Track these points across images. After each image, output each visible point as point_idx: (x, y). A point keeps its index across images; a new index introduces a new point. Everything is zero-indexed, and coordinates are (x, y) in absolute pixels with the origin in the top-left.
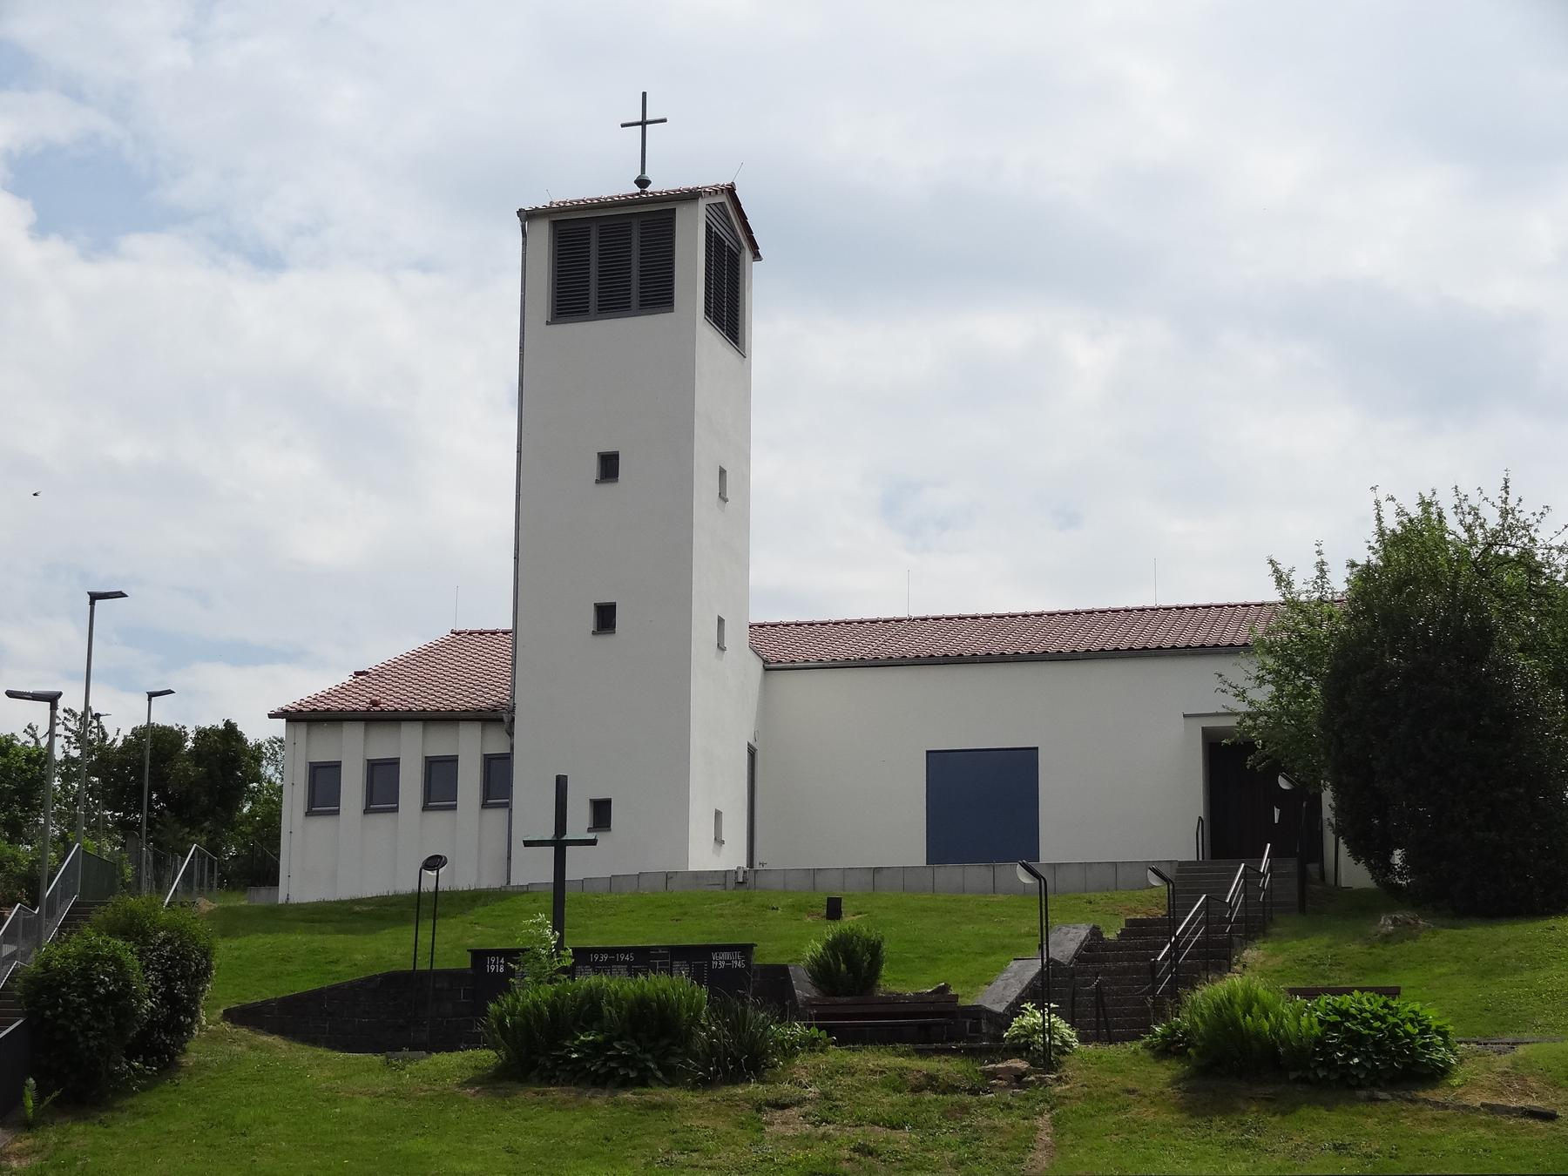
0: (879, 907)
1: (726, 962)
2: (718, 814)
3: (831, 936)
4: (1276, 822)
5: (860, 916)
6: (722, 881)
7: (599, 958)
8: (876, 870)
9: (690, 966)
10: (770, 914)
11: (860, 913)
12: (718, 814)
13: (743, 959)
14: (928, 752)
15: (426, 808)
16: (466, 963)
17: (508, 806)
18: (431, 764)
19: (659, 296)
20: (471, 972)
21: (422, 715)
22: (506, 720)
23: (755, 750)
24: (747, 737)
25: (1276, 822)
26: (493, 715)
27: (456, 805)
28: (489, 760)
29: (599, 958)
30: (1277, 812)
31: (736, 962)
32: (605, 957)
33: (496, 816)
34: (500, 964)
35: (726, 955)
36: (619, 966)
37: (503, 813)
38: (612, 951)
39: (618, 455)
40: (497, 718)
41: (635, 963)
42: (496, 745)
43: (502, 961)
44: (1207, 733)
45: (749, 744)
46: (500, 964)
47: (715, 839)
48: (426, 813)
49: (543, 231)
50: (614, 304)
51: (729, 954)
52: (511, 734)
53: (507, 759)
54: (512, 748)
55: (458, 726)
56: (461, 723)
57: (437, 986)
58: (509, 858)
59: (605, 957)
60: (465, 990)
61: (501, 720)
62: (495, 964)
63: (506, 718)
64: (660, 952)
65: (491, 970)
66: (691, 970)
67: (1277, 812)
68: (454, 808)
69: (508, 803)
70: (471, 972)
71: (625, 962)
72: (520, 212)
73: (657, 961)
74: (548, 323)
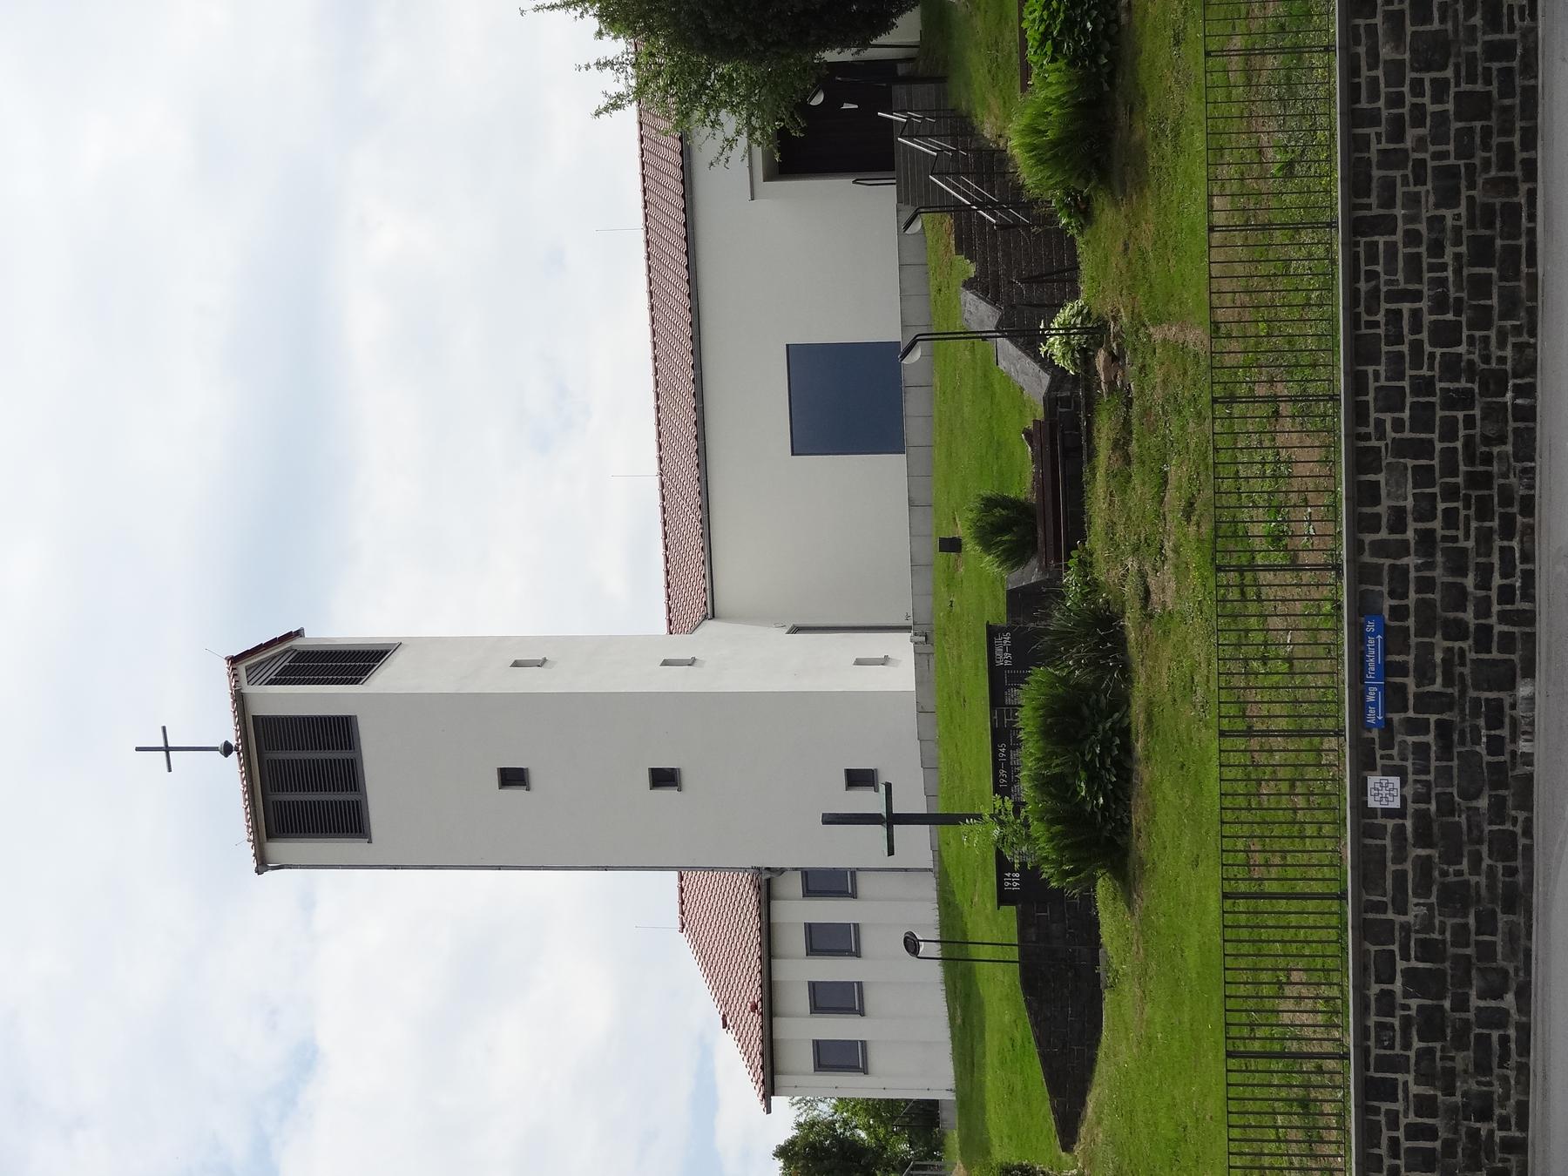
0: (948, 500)
1: (1004, 651)
2: (859, 662)
3: (977, 547)
4: (857, 107)
5: (957, 519)
6: (925, 656)
7: (1004, 778)
8: (911, 504)
10: (956, 609)
11: (955, 519)
12: (859, 662)
13: (1001, 636)
14: (792, 455)
15: (858, 954)
16: (1011, 911)
17: (854, 872)
19: (341, 730)
20: (1020, 906)
21: (765, 961)
22: (768, 876)
23: (794, 626)
24: (781, 634)
25: (857, 107)
26: (764, 889)
27: (854, 924)
28: (809, 892)
29: (1004, 778)
30: (846, 106)
31: (1005, 642)
32: (1002, 772)
33: (865, 884)
34: (1011, 877)
37: (859, 874)
38: (996, 765)
39: (501, 769)
40: (766, 885)
41: (1008, 743)
42: (794, 885)
43: (1008, 875)
45: (788, 633)
47: (883, 664)
48: (862, 955)
49: (279, 849)
50: (349, 775)
52: (782, 871)
53: (806, 874)
54: (796, 869)
55: (776, 923)
56: (771, 921)
57: (1034, 939)
58: (906, 870)
59: (1002, 772)
61: (769, 881)
62: (1011, 882)
64: (996, 717)
65: (1017, 886)
67: (846, 106)
68: (856, 926)
70: (1020, 906)
71: (1007, 752)
72: (259, 872)
74: (370, 842)
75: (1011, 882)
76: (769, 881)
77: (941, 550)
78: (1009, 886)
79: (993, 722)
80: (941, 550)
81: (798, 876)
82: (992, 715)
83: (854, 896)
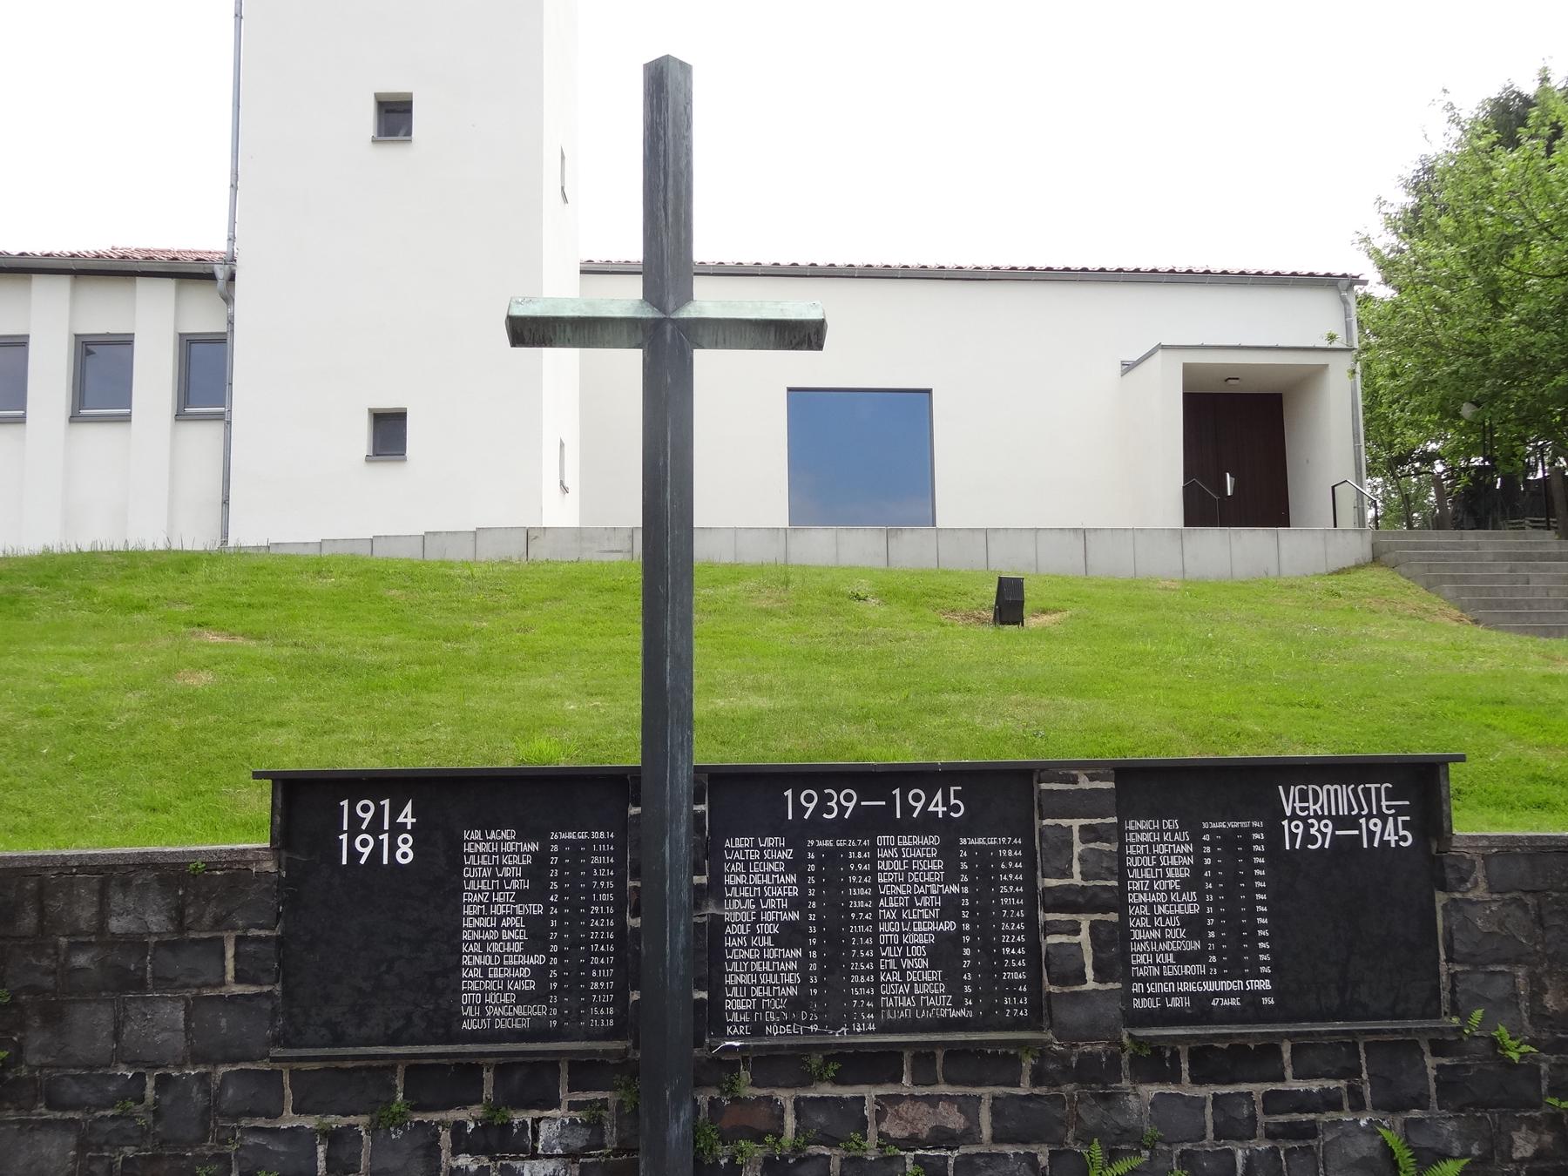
1: (1340, 822)
5: (1046, 617)
7: (822, 807)
9: (1196, 840)
11: (1044, 612)
13: (1400, 811)
14: (790, 390)
15: (74, 418)
17: (224, 419)
18: (86, 348)
20: (270, 866)
26: (198, 269)
27: (129, 415)
28: (189, 344)
29: (822, 807)
31: (1375, 825)
32: (845, 802)
33: (204, 436)
34: (397, 828)
35: (1338, 797)
36: (905, 841)
37: (213, 431)
41: (969, 826)
42: (202, 316)
43: (407, 817)
44: (1188, 369)
46: (397, 828)
48: (72, 424)
51: (1344, 792)
52: (228, 299)
53: (219, 342)
54: (231, 322)
56: (138, 279)
57: (116, 925)
58: (226, 502)
59: (845, 802)
60: (240, 940)
61: (211, 277)
63: (221, 273)
64: (1085, 784)
65: (354, 855)
66: (1199, 855)
68: (127, 419)
69: (222, 414)
70: (270, 866)
71: (927, 824)
73: (1076, 823)
75: (375, 828)
76: (211, 277)
77: (1002, 582)
78: (355, 821)
79: (1063, 770)
80: (1002, 582)
81: (221, 327)
82: (1093, 768)
83: (180, 416)
